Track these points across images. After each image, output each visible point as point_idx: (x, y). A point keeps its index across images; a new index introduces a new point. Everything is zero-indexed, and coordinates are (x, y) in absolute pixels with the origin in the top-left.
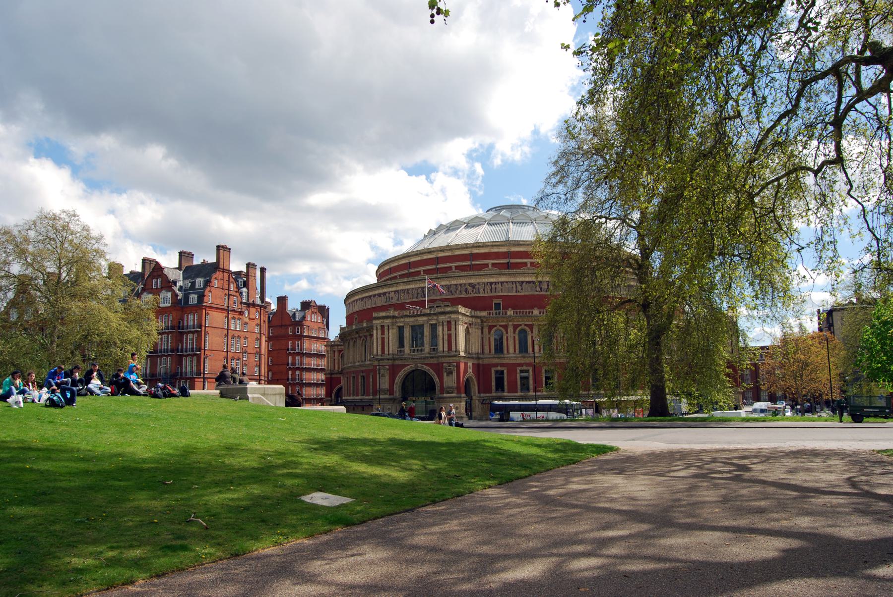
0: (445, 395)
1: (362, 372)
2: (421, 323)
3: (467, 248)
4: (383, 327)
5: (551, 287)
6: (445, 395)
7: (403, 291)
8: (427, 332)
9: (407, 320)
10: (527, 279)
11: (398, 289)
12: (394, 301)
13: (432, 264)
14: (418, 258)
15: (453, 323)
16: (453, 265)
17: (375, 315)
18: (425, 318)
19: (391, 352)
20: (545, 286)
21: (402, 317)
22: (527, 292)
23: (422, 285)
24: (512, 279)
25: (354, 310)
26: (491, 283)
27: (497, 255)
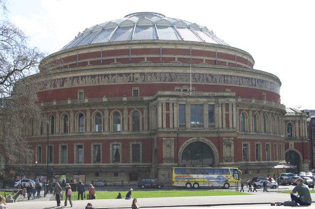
0: (225, 163)
1: (98, 141)
2: (202, 103)
3: (188, 44)
4: (168, 104)
5: (257, 83)
6: (225, 163)
7: (151, 74)
8: (206, 111)
9: (189, 100)
10: (246, 75)
12: (139, 82)
13: (157, 54)
15: (230, 106)
16: (176, 57)
17: (160, 93)
18: (205, 100)
19: (175, 126)
20: (254, 83)
21: (185, 97)
23: (170, 71)
24: (237, 74)
25: (76, 85)
26: (224, 76)
27: (209, 54)
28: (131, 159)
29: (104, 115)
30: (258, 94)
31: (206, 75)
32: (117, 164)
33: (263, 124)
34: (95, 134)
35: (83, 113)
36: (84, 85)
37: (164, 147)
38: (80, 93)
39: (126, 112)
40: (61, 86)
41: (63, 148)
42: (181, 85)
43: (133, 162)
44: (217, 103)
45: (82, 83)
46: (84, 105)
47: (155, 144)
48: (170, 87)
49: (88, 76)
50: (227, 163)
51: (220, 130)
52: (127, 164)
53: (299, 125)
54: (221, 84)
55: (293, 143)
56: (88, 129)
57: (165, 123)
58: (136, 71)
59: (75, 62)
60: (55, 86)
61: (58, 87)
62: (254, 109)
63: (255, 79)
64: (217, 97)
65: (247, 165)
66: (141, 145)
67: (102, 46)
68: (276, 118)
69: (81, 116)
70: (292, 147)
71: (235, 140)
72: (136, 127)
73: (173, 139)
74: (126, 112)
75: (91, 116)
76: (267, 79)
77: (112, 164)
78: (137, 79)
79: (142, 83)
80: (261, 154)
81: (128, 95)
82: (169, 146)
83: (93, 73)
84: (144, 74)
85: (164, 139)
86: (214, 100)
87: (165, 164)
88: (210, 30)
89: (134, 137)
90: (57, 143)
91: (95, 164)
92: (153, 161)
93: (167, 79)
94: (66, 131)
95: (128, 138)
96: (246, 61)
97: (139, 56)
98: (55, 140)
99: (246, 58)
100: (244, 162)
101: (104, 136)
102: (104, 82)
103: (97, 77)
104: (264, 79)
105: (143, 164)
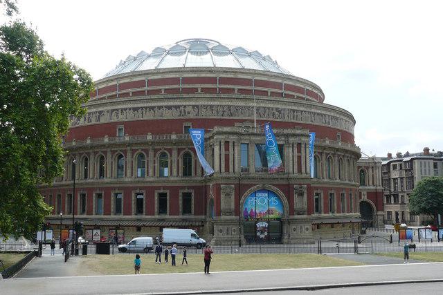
0: (296, 216)
4: (227, 143)
6: (296, 216)
7: (206, 107)
9: (253, 138)
10: (318, 111)
11: (197, 104)
12: (192, 116)
14: (196, 75)
15: (303, 146)
16: (237, 87)
17: (216, 129)
19: (236, 170)
22: (318, 122)
23: (230, 104)
24: (308, 110)
25: (115, 119)
26: (294, 111)
28: (181, 210)
29: (148, 156)
30: (333, 133)
31: (272, 108)
32: (163, 216)
33: (337, 169)
34: (137, 179)
35: (122, 153)
36: (124, 120)
37: (222, 196)
38: (120, 129)
39: (175, 153)
40: (97, 121)
41: (98, 197)
42: (242, 121)
43: (183, 215)
44: (288, 142)
45: (122, 118)
46: (124, 144)
47: (211, 192)
48: (230, 123)
49: (130, 109)
50: (300, 216)
51: (291, 176)
52: (176, 217)
53: (373, 172)
54: (290, 121)
55: (365, 193)
56: (129, 174)
57: (223, 165)
58: (188, 103)
59: (114, 93)
60: (89, 120)
61: (93, 122)
62: (327, 152)
63: (329, 116)
64: (287, 136)
65: (319, 218)
66: (193, 194)
67: (148, 74)
68: (351, 163)
69: (120, 156)
70: (365, 198)
71: (309, 189)
72: (187, 171)
73: (233, 186)
74: (175, 153)
75: (132, 156)
76: (341, 117)
77: (157, 216)
78: (189, 113)
79: (195, 117)
80: (335, 204)
81: (178, 132)
82: (228, 195)
83: (136, 106)
84: (197, 106)
85: (221, 186)
86: (283, 139)
87: (223, 217)
88: (274, 60)
89: (184, 184)
90: (91, 190)
91: (136, 216)
92: (208, 214)
93: (226, 113)
94: (102, 174)
95: (177, 185)
96: (316, 96)
97: (191, 86)
98: (90, 186)
99: (316, 92)
100: (316, 215)
101: (147, 182)
102: (149, 116)
103: (140, 111)
104: (338, 116)
105: (197, 217)
